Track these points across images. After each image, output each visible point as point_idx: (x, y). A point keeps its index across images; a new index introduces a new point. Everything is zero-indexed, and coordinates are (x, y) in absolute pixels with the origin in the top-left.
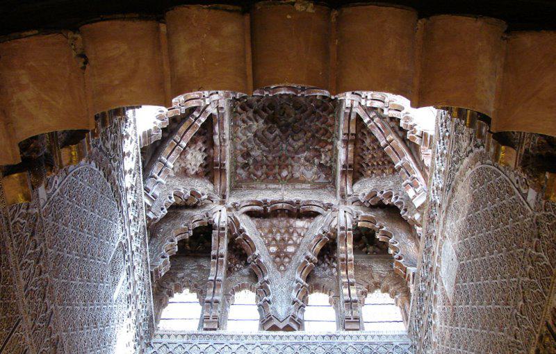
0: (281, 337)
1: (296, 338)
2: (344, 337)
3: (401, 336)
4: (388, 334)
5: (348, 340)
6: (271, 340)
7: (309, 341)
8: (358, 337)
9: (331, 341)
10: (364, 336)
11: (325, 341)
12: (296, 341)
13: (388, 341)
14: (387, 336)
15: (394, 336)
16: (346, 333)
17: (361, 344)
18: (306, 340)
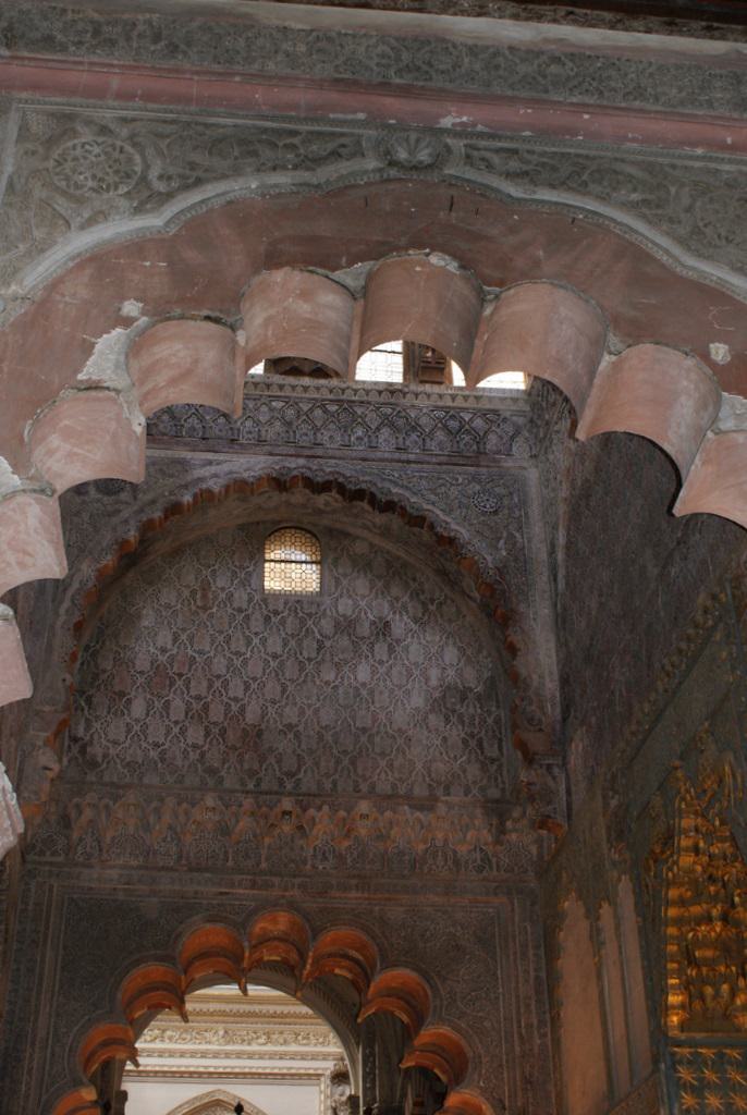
0: (306, 389)
1: (331, 392)
2: (417, 395)
3: (515, 400)
4: (493, 395)
5: (422, 402)
6: (288, 392)
7: (353, 398)
8: (441, 396)
9: (392, 400)
10: (451, 395)
11: (382, 400)
12: (331, 397)
13: (492, 407)
14: (490, 399)
15: (503, 399)
16: (421, 388)
17: (447, 409)
18: (349, 395)
